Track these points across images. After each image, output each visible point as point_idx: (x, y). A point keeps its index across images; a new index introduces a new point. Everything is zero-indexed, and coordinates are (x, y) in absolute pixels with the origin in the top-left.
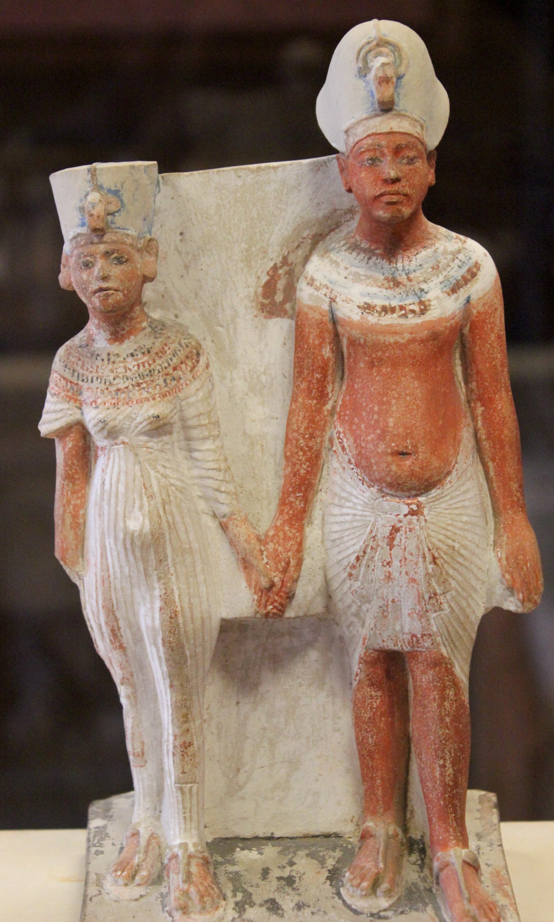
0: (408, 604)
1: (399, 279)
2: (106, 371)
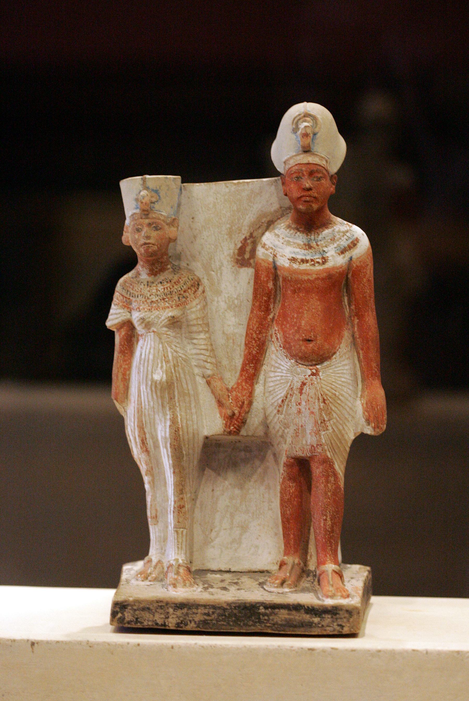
0: (309, 427)
1: (312, 245)
2: (146, 291)
